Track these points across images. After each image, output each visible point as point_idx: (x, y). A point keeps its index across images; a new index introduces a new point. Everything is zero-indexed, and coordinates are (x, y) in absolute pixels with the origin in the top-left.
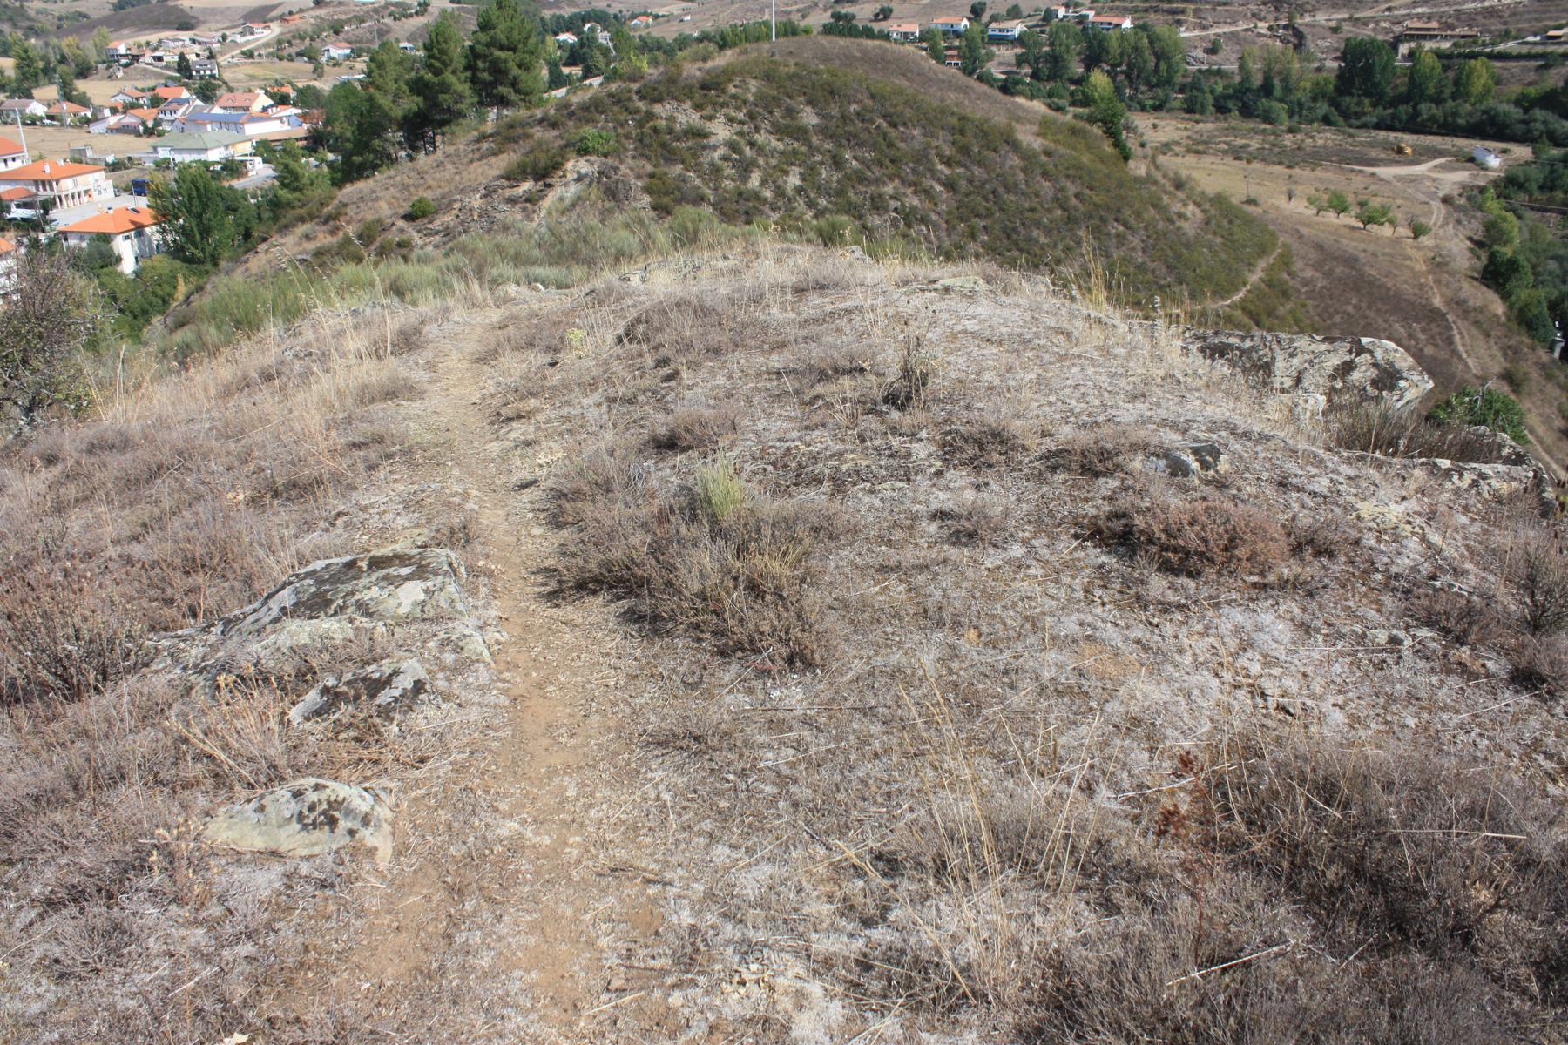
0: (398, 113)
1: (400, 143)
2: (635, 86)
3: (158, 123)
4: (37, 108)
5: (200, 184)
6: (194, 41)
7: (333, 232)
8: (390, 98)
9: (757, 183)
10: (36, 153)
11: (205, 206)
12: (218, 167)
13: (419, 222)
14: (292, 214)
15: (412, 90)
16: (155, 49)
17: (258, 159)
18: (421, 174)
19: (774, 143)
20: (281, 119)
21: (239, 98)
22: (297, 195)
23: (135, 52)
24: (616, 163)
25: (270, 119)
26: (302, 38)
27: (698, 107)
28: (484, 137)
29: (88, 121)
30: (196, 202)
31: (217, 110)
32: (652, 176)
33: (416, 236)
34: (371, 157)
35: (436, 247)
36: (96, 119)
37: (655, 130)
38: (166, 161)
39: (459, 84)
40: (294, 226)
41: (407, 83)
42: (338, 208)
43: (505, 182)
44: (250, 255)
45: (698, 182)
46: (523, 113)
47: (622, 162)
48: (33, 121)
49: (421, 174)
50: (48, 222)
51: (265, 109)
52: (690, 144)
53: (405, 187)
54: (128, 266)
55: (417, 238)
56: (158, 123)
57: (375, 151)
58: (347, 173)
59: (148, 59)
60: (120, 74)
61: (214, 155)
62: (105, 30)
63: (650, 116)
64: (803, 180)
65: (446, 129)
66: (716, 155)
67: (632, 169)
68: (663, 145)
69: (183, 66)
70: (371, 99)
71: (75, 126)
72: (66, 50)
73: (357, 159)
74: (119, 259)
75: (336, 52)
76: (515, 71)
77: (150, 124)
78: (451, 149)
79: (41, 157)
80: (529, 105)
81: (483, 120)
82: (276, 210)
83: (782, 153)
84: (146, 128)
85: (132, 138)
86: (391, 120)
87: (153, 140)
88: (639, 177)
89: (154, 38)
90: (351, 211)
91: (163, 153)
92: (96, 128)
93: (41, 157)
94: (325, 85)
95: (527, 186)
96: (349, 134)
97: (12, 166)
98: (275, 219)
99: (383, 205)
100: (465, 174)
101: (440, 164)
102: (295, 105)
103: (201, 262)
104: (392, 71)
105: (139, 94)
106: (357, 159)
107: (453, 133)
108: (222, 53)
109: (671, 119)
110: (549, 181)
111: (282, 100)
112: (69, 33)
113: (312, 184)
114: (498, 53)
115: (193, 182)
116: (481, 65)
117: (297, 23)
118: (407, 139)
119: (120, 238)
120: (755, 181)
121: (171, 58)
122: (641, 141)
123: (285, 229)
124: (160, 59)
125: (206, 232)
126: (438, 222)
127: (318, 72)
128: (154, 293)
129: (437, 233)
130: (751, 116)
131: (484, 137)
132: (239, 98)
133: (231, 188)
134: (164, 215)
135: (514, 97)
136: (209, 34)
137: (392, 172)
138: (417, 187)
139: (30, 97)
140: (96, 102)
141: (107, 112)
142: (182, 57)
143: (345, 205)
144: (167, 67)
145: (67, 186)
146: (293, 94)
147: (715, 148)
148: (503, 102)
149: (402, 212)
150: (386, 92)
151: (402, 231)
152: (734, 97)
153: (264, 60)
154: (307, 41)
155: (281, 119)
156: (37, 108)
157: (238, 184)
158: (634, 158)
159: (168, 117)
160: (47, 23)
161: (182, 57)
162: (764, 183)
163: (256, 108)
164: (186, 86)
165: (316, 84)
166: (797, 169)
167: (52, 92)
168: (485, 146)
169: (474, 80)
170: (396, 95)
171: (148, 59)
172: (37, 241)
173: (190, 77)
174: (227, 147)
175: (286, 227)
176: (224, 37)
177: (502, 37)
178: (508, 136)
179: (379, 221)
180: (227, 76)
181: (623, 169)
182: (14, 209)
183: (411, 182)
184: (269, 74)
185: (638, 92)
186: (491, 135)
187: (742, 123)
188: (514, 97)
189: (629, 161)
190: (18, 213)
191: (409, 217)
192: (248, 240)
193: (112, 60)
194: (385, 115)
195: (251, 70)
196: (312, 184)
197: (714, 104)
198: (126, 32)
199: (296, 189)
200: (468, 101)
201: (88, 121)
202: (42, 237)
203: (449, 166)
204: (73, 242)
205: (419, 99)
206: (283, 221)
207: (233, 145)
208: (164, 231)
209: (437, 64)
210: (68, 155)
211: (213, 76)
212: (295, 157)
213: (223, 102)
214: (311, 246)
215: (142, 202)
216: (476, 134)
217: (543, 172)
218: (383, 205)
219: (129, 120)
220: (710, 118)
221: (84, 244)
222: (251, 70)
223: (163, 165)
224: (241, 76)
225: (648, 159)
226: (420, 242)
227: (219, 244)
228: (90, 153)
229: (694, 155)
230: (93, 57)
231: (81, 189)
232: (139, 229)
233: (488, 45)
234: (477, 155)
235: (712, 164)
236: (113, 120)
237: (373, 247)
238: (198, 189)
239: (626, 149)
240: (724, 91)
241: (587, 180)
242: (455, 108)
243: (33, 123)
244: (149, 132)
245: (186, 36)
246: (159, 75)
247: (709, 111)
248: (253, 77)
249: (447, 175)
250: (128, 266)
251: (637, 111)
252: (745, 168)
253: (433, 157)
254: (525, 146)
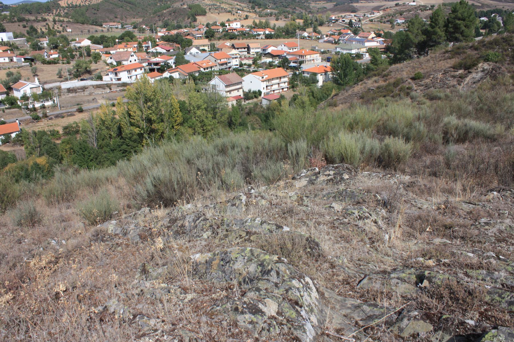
0: (416, 41)
1: (415, 52)
3: (339, 40)
4: (306, 34)
5: (347, 60)
6: (355, 16)
7: (385, 81)
8: (414, 35)
10: (302, 47)
11: (347, 67)
12: (354, 55)
13: (416, 81)
14: (373, 73)
15: (422, 33)
16: (343, 18)
17: (367, 54)
18: (421, 64)
20: (377, 41)
21: (365, 34)
22: (376, 66)
23: (337, 19)
24: (500, 66)
25: (374, 41)
26: (389, 16)
28: (447, 52)
29: (319, 39)
30: (344, 66)
31: (358, 37)
33: (414, 86)
34: (404, 56)
35: (421, 91)
36: (321, 38)
38: (339, 52)
39: (441, 32)
40: (372, 77)
41: (421, 31)
42: (388, 72)
43: (452, 69)
44: (356, 85)
46: (464, 44)
47: (503, 65)
48: (304, 38)
49: (421, 64)
50: (300, 68)
51: (373, 38)
53: (414, 68)
54: (320, 84)
55: (415, 87)
56: (339, 40)
57: (405, 54)
58: (395, 61)
59: (340, 21)
60: (331, 25)
61: (354, 52)
62: (329, 12)
65: (433, 48)
69: (351, 23)
70: (407, 35)
71: (315, 40)
72: (318, 18)
73: (399, 56)
74: (318, 81)
75: (399, 21)
76: (463, 28)
77: (336, 40)
78: (433, 55)
79: (303, 48)
80: (467, 41)
81: (447, 46)
82: (368, 71)
84: (335, 41)
85: (330, 45)
86: (413, 43)
87: (336, 46)
89: (343, 15)
90: (393, 74)
91: (338, 50)
92: (321, 41)
93: (303, 48)
94: (393, 32)
95: (461, 71)
96: (397, 47)
97: (294, 50)
98: (366, 74)
99: (405, 73)
100: (437, 65)
101: (428, 61)
102: (383, 38)
103: (342, 85)
104: (416, 26)
105: (335, 31)
106: (399, 56)
107: (435, 50)
108: (363, 20)
110: (470, 70)
111: (379, 35)
112: (320, 13)
113: (381, 63)
114: (457, 22)
115: (345, 59)
116: (450, 25)
117: (389, 11)
118: (418, 51)
119: (319, 75)
121: (347, 21)
123: (369, 78)
124: (344, 21)
125: (346, 75)
126: (424, 82)
127: (393, 27)
128: (325, 93)
129: (422, 86)
131: (447, 52)
132: (365, 34)
133: (356, 62)
134: (334, 69)
135: (461, 38)
136: (360, 14)
137: (410, 62)
138: (418, 68)
139: (305, 31)
140: (323, 33)
141: (325, 36)
142: (351, 21)
143: (391, 72)
144: (346, 24)
145: (308, 57)
146: (383, 34)
148: (456, 40)
149: (411, 76)
150: (413, 33)
151: (409, 83)
153: (376, 23)
154: (391, 17)
155: (377, 41)
156: (306, 34)
157: (359, 61)
159: (342, 39)
160: (315, 10)
161: (351, 21)
163: (370, 37)
164: (350, 30)
165: (391, 31)
167: (311, 30)
168: (447, 55)
169: (446, 31)
170: (416, 35)
171: (340, 21)
172: (296, 73)
173: (352, 27)
174: (358, 49)
175: (369, 77)
176: (365, 15)
177: (460, 15)
178: (456, 52)
179: (402, 79)
180: (363, 27)
182: (292, 63)
183: (416, 66)
184: (376, 27)
186: (450, 51)
188: (461, 38)
189: (506, 66)
190: (292, 64)
191: (413, 79)
192: (358, 80)
193: (330, 21)
194: (411, 41)
195: (371, 26)
196: (381, 63)
198: (336, 13)
199: (376, 65)
200: (443, 38)
201: (319, 39)
202: (297, 72)
203: (431, 62)
204: (305, 75)
205: (425, 37)
206: (369, 75)
207: (360, 49)
208: (333, 74)
209: (433, 24)
210: (311, 48)
211: (359, 27)
212: (377, 54)
213: (360, 35)
214: (376, 85)
215: (328, 64)
216: (444, 50)
217: (469, 67)
218: (405, 73)
219: (331, 39)
221: (308, 76)
222: (371, 26)
223: (337, 53)
224: (368, 27)
226: (415, 88)
227: (349, 80)
228: (317, 48)
230: (325, 20)
231: (312, 59)
232: (326, 72)
233: (454, 18)
234: (443, 58)
236: (326, 39)
237: (398, 88)
238: (345, 62)
239: (505, 60)
241: (486, 72)
242: (437, 40)
243: (304, 39)
244: (336, 43)
245: (353, 14)
246: (343, 26)
248: (371, 28)
249: (430, 65)
250: (320, 84)
253: (426, 58)
254: (463, 56)
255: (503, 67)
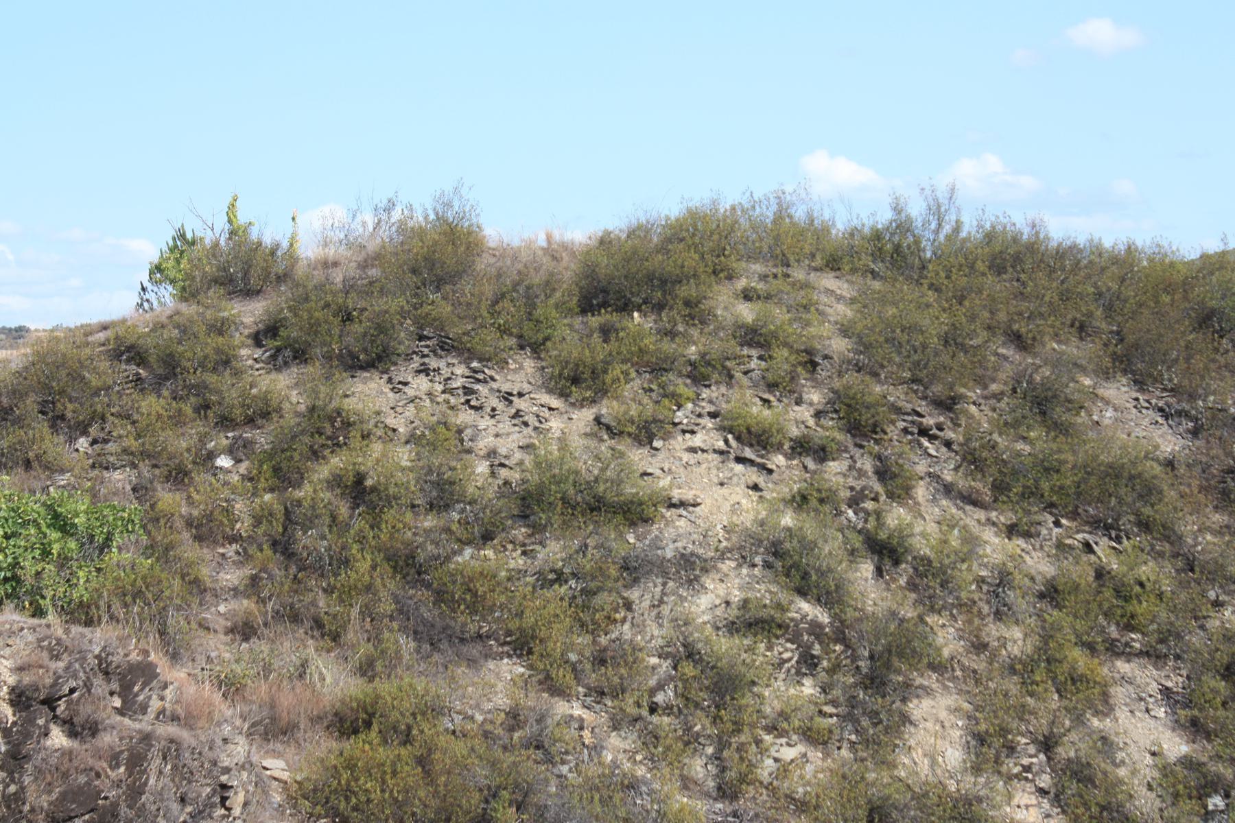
2: (250, 313)
9: (954, 756)
19: (995, 547)
27: (575, 382)
32: (348, 723)
37: (357, 490)
45: (618, 748)
52: (553, 551)
63: (331, 428)
64: (1195, 729)
66: (708, 602)
67: (231, 687)
68: (407, 565)
83: (1051, 593)
88: (273, 729)
109: (441, 439)
120: (935, 739)
122: (283, 547)
130: (859, 423)
147: (690, 569)
152: (753, 337)
158: (244, 630)
162: (989, 746)
166: (1147, 676)
181: (179, 682)
185: (267, 333)
187: (801, 447)
189: (218, 646)
197: (658, 368)
220: (647, 433)
225: (329, 633)
229: (586, 615)
235: (687, 653)
239: (196, 587)
240: (696, 312)
247: (631, 398)
251: (262, 413)
252: (876, 677)
255: (176, 675)
